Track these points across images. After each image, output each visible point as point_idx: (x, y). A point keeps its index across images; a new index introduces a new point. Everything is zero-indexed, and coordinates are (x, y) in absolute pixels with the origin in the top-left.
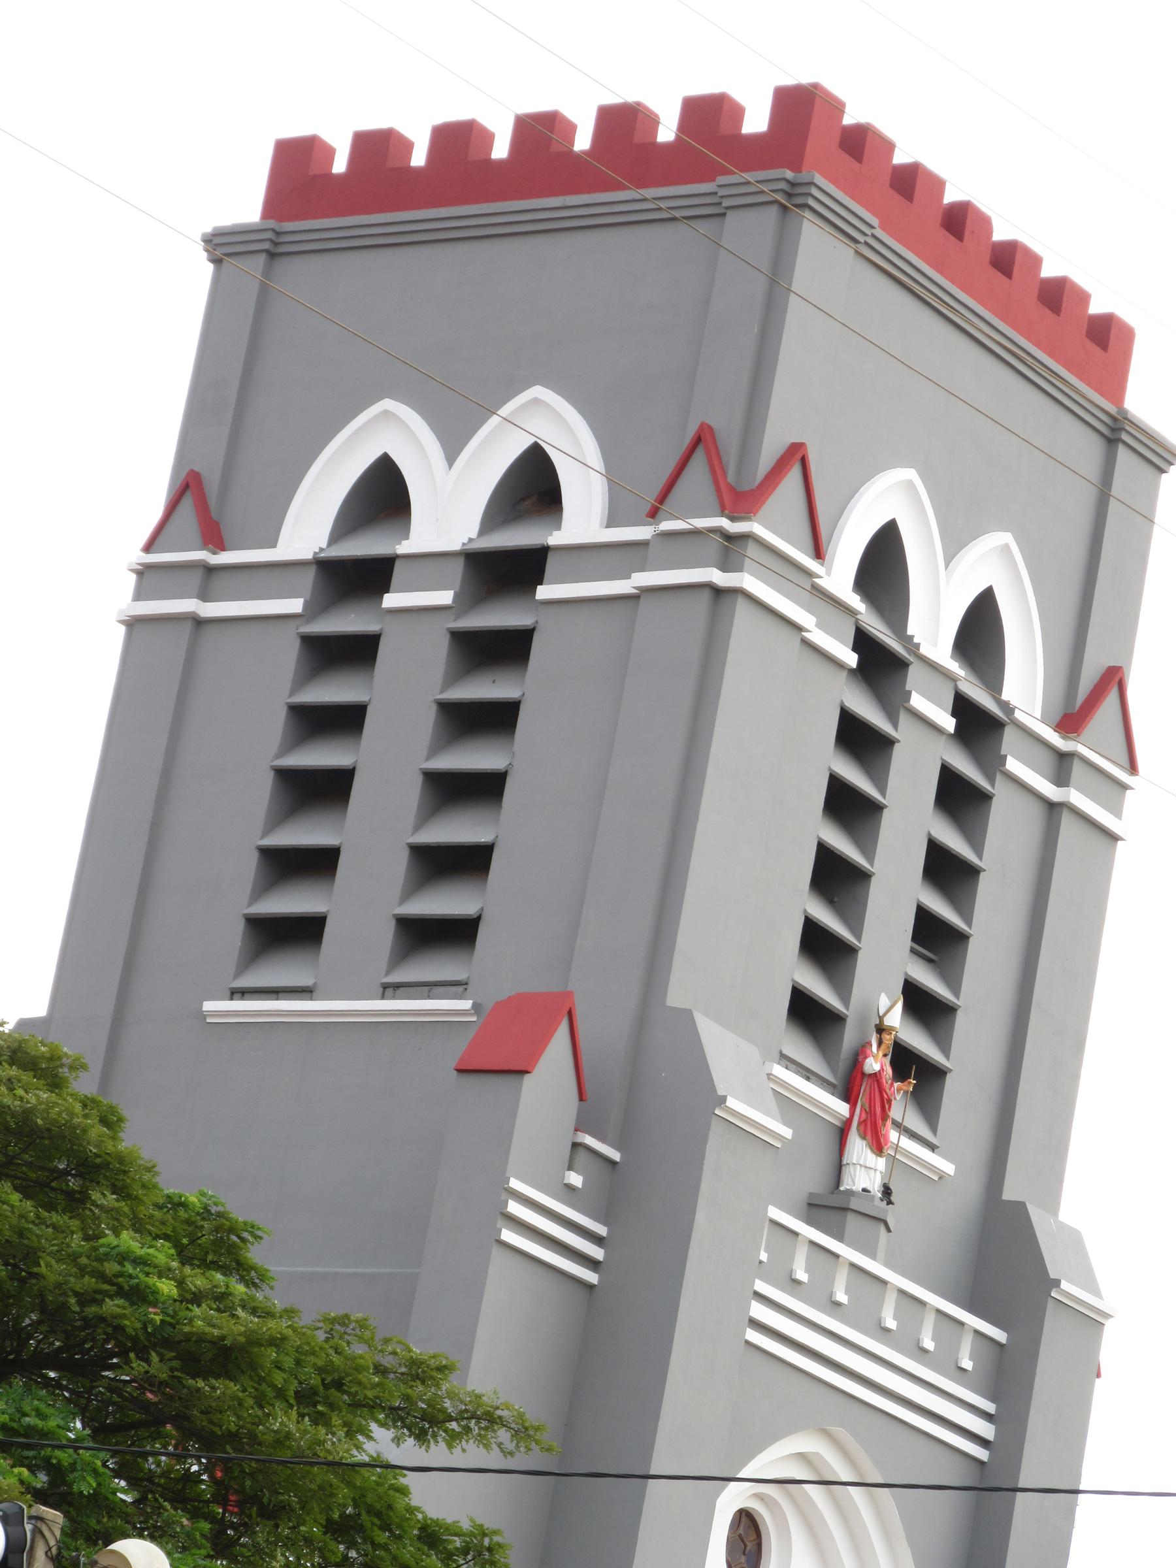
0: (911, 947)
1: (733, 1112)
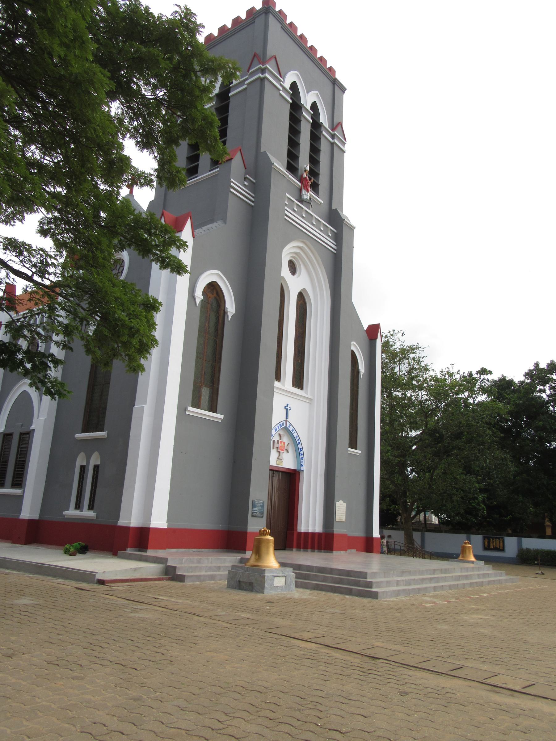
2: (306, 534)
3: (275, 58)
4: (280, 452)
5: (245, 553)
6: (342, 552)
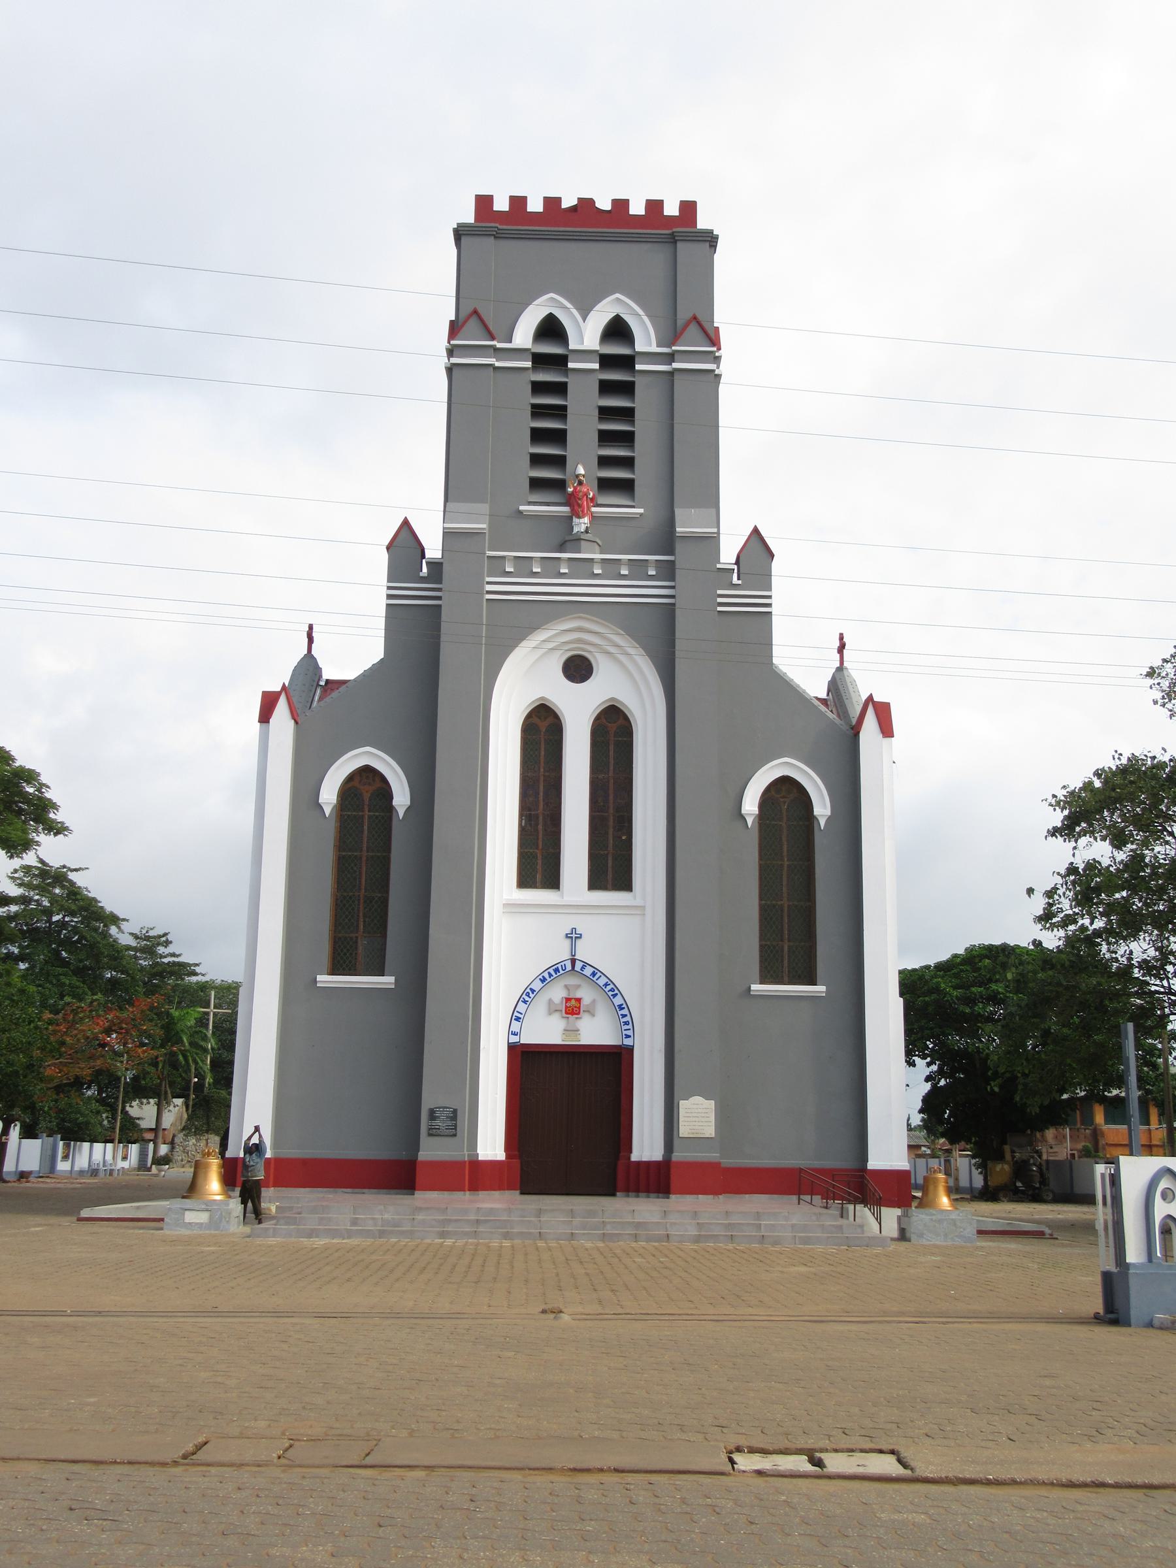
2: (639, 1163)
3: (475, 312)
4: (568, 1018)
5: (414, 1194)
6: (700, 1196)
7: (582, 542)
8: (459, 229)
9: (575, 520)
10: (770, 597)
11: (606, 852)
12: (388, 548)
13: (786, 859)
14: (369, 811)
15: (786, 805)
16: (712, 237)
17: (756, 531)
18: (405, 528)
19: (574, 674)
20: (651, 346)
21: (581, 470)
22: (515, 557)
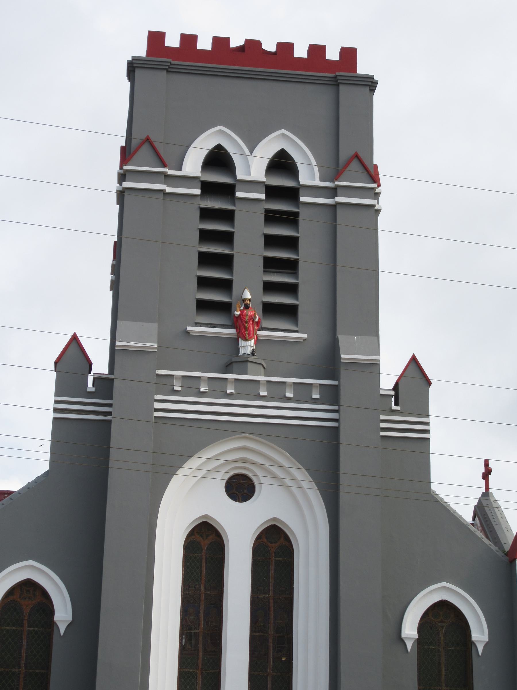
0: (264, 270)
1: (141, 347)
7: (249, 364)
8: (134, 62)
9: (242, 343)
10: (427, 424)
11: (266, 673)
12: (56, 363)
13: (444, 685)
14: (28, 627)
15: (444, 629)
16: (372, 82)
17: (414, 359)
18: (74, 344)
19: (237, 492)
20: (315, 180)
21: (247, 295)
22: (184, 377)
